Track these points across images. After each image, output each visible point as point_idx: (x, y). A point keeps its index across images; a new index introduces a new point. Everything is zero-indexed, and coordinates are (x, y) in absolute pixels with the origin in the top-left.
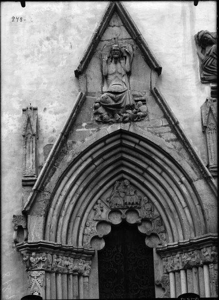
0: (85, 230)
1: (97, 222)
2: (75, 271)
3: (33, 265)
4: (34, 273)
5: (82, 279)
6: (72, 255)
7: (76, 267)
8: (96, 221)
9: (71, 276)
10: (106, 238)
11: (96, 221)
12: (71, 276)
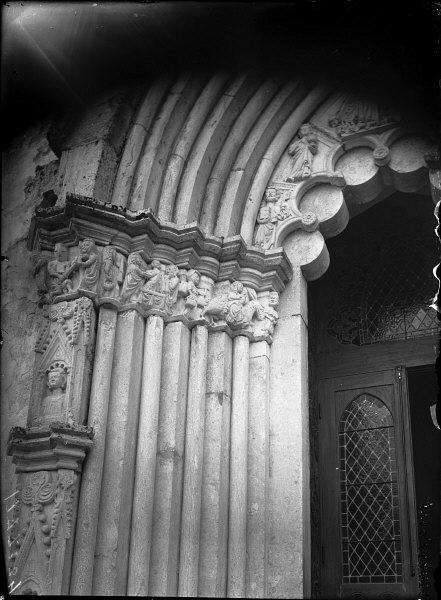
0: (263, 210)
1: (299, 185)
2: (216, 315)
3: (55, 283)
4: (61, 309)
5: (242, 343)
6: (205, 263)
7: (215, 303)
8: (297, 180)
9: (202, 331)
10: (324, 228)
11: (297, 180)
12: (202, 331)
